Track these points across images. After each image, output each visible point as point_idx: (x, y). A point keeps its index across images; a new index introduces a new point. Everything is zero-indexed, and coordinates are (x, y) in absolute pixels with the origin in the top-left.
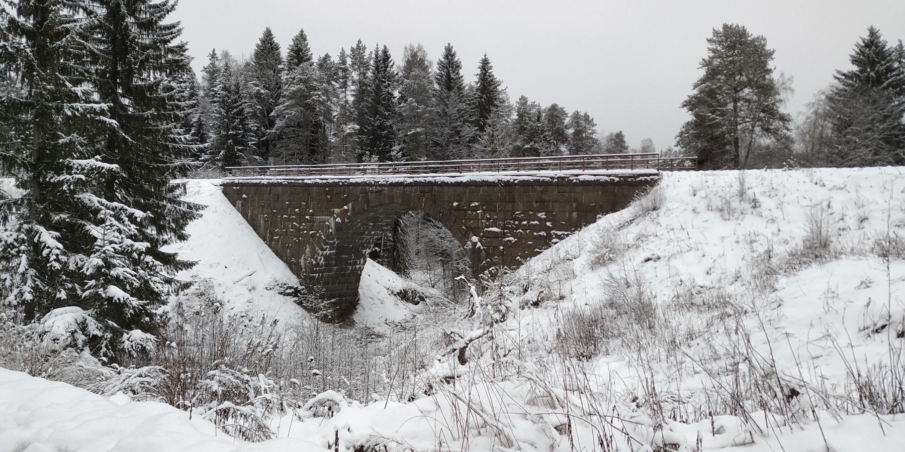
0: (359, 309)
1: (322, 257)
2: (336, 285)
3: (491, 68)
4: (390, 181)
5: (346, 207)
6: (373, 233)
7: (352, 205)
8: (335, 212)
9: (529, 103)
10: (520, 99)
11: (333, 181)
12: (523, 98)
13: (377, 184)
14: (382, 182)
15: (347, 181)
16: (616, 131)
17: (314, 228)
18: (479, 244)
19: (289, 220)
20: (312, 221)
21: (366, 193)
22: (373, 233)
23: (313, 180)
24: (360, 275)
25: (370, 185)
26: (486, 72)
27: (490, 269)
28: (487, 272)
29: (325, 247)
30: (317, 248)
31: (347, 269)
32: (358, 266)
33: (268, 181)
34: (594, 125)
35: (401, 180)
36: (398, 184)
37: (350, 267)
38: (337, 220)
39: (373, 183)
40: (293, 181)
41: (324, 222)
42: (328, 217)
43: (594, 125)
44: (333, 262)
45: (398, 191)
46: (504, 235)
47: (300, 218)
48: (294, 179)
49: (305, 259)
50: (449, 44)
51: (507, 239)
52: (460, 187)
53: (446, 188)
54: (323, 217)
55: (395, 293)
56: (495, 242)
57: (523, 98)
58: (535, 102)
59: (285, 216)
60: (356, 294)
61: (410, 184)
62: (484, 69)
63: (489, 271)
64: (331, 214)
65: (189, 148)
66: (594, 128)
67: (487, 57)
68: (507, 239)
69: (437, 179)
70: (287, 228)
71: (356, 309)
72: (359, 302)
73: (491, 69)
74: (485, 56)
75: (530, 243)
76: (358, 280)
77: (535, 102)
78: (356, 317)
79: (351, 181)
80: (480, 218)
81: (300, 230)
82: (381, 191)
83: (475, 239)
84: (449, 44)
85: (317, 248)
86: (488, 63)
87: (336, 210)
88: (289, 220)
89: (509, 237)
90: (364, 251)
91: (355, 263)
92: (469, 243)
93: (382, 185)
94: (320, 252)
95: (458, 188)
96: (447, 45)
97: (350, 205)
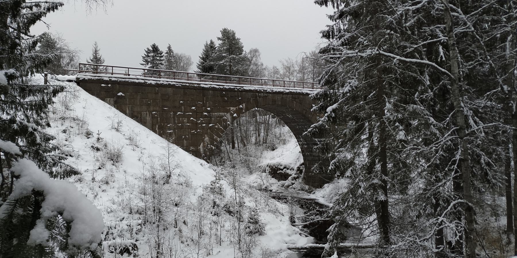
4: (275, 90)
5: (241, 106)
8: (231, 110)
11: (229, 87)
13: (265, 92)
14: (269, 90)
15: (241, 88)
19: (184, 116)
20: (210, 117)
23: (209, 86)
25: (260, 92)
30: (215, 137)
33: (155, 82)
35: (282, 90)
36: (279, 93)
39: (262, 90)
40: (187, 84)
41: (222, 117)
42: (226, 114)
45: (279, 97)
47: (197, 114)
48: (188, 83)
49: (204, 147)
54: (221, 113)
59: (179, 113)
61: (287, 93)
64: (228, 111)
69: (303, 91)
70: (183, 122)
79: (244, 88)
81: (197, 124)
82: (267, 96)
85: (215, 137)
87: (232, 108)
88: (184, 116)
93: (269, 93)
97: (244, 105)
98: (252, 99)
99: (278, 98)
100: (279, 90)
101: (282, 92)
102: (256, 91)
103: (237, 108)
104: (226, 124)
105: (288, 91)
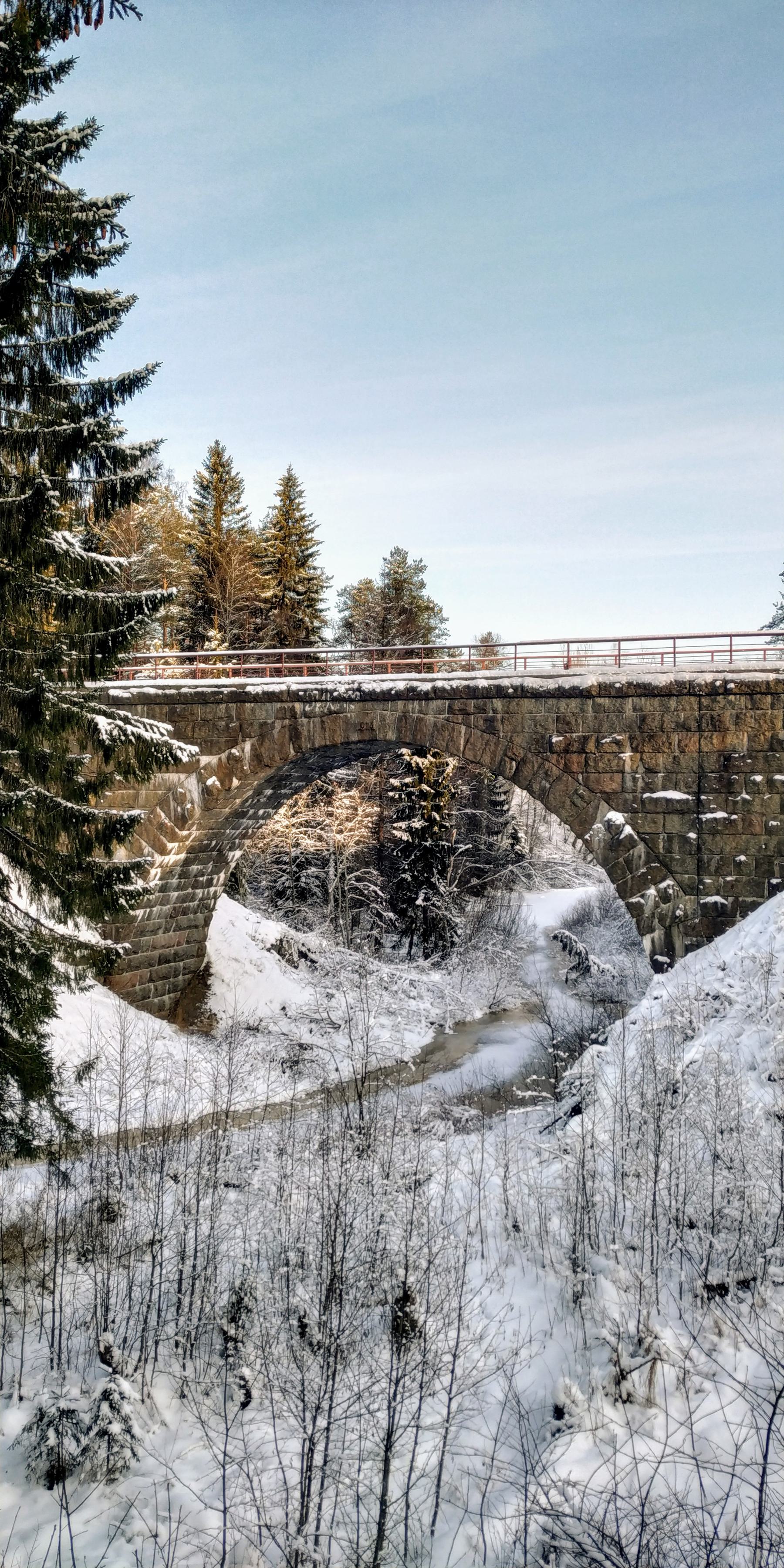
0: (216, 986)
1: (159, 870)
2: (171, 933)
3: (300, 494)
4: (366, 687)
6: (261, 812)
7: (253, 745)
8: (202, 763)
9: (410, 561)
10: (392, 555)
12: (397, 552)
16: (484, 633)
17: (142, 800)
18: (628, 830)
21: (294, 716)
22: (261, 812)
23: (135, 691)
24: (213, 909)
25: (306, 698)
26: (291, 501)
27: (663, 885)
28: (652, 892)
29: (170, 846)
31: (193, 898)
32: (212, 889)
34: (443, 620)
36: (386, 697)
37: (199, 892)
38: (209, 782)
42: (183, 776)
43: (443, 620)
44: (175, 881)
46: (700, 806)
50: (217, 442)
51: (709, 816)
52: (568, 701)
53: (527, 704)
55: (269, 946)
56: (674, 823)
57: (397, 552)
58: (421, 561)
60: (201, 952)
62: (289, 498)
63: (658, 891)
65: (99, 564)
66: (442, 626)
67: (293, 472)
68: (709, 816)
71: (208, 987)
72: (212, 971)
73: (300, 496)
74: (289, 470)
75: (774, 823)
76: (207, 922)
77: (421, 561)
78: (213, 1004)
80: (627, 768)
83: (617, 817)
84: (217, 442)
86: (295, 485)
89: (712, 811)
90: (231, 854)
91: (210, 883)
92: (598, 826)
93: (340, 699)
94: (158, 858)
95: (563, 703)
96: (213, 445)
97: (248, 746)
98: (278, 725)
99: (383, 718)
100: (386, 686)
101: (383, 692)
102: (293, 696)
103: (224, 756)
104: (183, 809)
105: (427, 687)
